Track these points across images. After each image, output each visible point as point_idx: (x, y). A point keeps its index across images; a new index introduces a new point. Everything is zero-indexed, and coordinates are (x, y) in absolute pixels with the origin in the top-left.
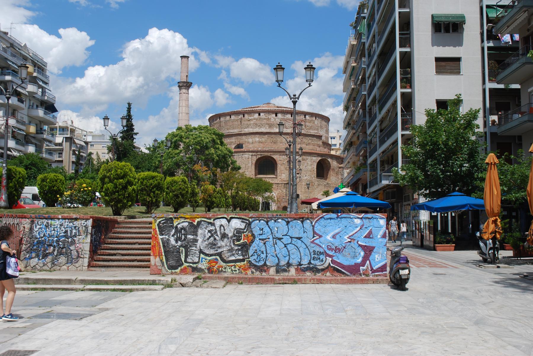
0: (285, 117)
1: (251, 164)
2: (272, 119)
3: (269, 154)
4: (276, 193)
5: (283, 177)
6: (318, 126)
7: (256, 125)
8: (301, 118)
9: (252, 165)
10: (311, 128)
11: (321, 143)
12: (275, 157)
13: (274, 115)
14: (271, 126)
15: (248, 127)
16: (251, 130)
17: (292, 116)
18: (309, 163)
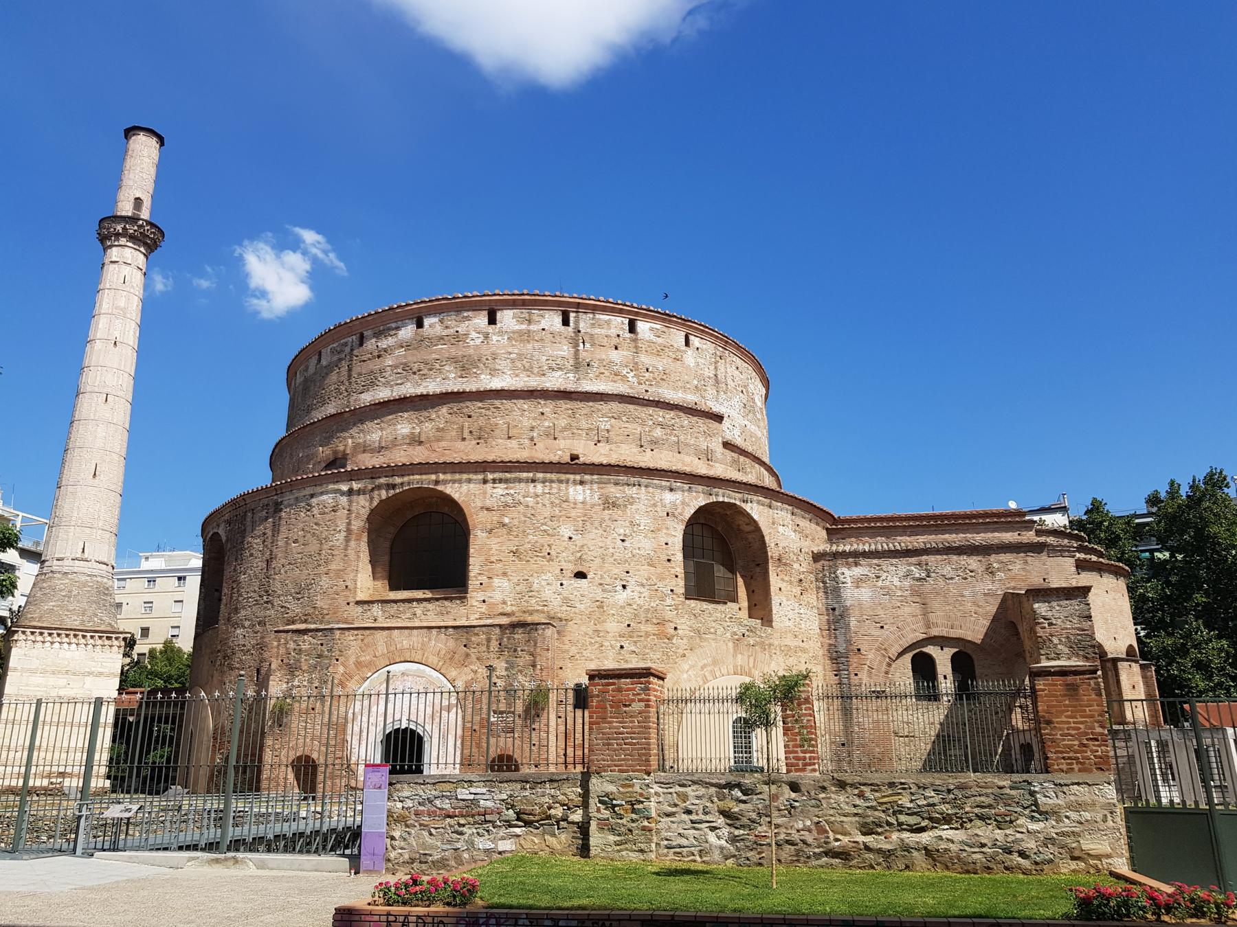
2: (474, 335)
3: (426, 481)
5: (498, 596)
6: (702, 378)
8: (613, 332)
9: (347, 540)
10: (664, 376)
11: (719, 449)
12: (460, 490)
13: (481, 320)
14: (466, 366)
15: (372, 384)
16: (383, 394)
17: (566, 322)
18: (644, 521)
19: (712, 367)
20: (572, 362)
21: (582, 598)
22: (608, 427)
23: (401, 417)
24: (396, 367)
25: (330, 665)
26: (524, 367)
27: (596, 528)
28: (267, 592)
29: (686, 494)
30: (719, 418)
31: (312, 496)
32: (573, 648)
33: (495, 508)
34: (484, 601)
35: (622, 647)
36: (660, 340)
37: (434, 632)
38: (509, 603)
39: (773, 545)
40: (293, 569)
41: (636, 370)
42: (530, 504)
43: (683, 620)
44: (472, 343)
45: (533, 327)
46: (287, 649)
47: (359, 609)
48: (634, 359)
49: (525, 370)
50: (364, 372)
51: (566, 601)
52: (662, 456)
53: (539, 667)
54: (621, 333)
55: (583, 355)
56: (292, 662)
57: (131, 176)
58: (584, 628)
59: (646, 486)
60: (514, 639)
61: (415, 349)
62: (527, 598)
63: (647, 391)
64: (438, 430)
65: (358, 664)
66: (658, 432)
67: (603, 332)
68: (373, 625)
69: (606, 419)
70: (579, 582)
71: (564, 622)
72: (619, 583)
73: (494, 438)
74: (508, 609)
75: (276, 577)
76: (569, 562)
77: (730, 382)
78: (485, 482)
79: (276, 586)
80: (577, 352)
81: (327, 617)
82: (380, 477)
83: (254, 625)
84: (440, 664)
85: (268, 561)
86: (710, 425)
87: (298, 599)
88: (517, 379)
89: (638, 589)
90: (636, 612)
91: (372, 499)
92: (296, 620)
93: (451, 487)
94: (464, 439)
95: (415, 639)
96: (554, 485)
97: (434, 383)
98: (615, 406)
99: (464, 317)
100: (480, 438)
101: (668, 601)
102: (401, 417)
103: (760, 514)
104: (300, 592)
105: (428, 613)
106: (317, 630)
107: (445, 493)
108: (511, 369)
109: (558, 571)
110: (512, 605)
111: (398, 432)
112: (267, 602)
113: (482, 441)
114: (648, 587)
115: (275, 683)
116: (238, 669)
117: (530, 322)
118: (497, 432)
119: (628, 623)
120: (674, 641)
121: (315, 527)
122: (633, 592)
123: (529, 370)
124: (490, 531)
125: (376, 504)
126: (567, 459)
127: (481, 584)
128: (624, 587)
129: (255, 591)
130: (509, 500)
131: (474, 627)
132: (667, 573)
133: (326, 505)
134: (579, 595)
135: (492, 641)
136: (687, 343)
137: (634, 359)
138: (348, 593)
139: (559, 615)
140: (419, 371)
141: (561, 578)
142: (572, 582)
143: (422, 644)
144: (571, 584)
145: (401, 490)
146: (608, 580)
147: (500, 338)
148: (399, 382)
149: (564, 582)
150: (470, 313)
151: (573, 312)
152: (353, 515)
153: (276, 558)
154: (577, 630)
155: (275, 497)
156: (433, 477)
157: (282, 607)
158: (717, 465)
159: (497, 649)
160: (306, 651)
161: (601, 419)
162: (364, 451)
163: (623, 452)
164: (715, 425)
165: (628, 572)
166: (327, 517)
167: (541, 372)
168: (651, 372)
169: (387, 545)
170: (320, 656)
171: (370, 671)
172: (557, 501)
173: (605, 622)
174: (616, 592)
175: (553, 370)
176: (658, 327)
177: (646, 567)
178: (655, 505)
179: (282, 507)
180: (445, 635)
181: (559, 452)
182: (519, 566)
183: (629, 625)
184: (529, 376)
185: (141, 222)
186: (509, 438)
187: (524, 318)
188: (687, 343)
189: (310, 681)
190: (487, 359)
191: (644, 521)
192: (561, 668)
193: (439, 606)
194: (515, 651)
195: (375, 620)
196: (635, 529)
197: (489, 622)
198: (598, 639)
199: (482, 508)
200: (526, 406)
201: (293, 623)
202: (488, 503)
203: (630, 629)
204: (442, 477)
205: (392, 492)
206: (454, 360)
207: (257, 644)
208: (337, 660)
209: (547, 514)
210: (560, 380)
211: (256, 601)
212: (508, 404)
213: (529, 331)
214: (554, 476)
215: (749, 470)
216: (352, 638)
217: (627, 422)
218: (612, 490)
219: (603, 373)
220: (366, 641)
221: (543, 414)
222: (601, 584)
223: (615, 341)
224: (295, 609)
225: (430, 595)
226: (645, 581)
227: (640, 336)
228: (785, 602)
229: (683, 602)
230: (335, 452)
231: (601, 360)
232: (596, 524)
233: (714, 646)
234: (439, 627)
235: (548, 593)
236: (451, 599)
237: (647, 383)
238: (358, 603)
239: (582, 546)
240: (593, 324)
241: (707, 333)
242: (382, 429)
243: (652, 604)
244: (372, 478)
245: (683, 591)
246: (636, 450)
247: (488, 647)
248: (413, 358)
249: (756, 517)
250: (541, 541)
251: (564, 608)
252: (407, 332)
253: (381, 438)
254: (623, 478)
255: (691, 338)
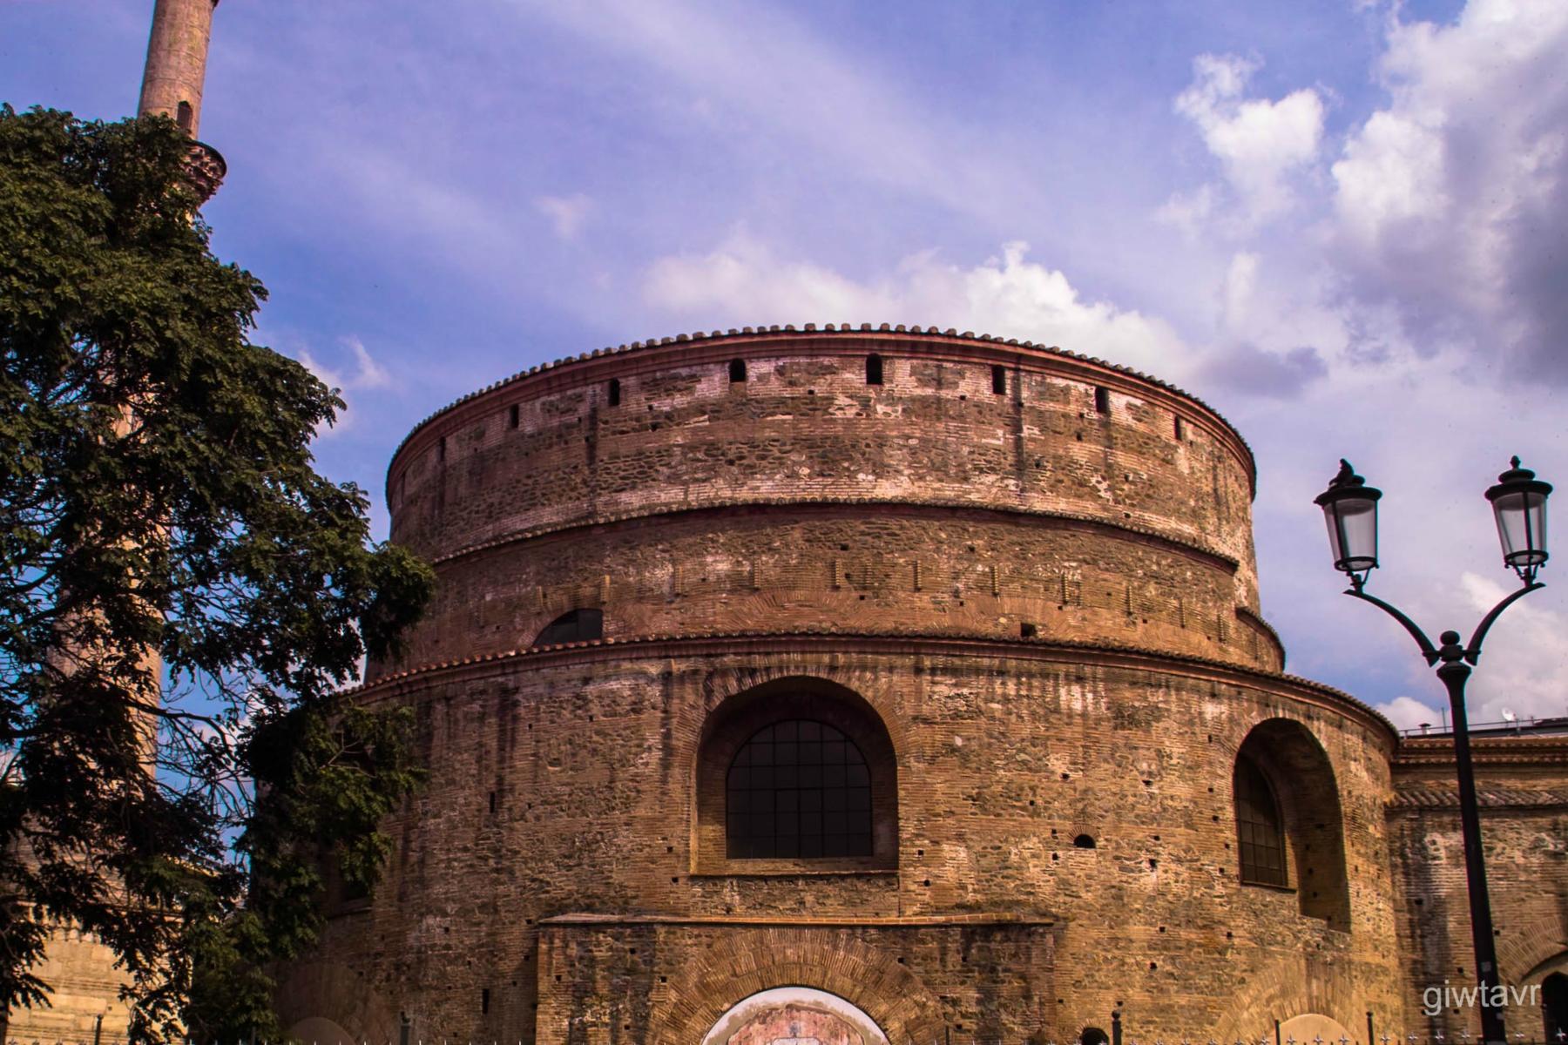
0: (946, 394)
1: (657, 755)
2: (842, 400)
3: (812, 665)
4: (895, 1025)
5: (949, 875)
6: (1199, 496)
7: (714, 457)
8: (1073, 409)
9: (665, 765)
10: (1148, 494)
11: (1232, 623)
13: (855, 377)
15: (642, 474)
16: (669, 496)
17: (998, 388)
18: (1176, 749)
19: (1210, 477)
20: (1011, 458)
21: (1088, 882)
22: (1078, 577)
23: (712, 540)
24: (693, 448)
25: (651, 989)
26: (933, 464)
27: (1106, 761)
28: (496, 851)
29: (1234, 705)
30: (1230, 565)
31: (586, 681)
32: (1079, 967)
33: (938, 720)
34: (927, 883)
35: (1153, 966)
36: (1141, 427)
37: (843, 934)
38: (970, 888)
39: (1345, 793)
40: (552, 812)
41: (1111, 478)
42: (997, 715)
43: (1239, 922)
44: (839, 414)
45: (946, 394)
46: (567, 957)
47: (698, 890)
48: (1106, 456)
49: (934, 468)
50: (623, 451)
51: (1064, 885)
52: (1160, 632)
53: (1036, 999)
54: (1085, 411)
55: (1031, 446)
56: (578, 980)
57: (174, 61)
58: (1094, 933)
59: (1178, 690)
60: (989, 950)
61: (730, 418)
62: (999, 879)
63: (1127, 516)
64: (786, 568)
65: (705, 988)
66: (1152, 590)
67: (1059, 407)
68: (727, 920)
69: (1074, 564)
70: (1083, 853)
71: (1062, 923)
72: (1144, 856)
73: (891, 590)
74: (970, 897)
75: (517, 825)
76: (1066, 818)
77: (1230, 498)
78: (918, 671)
79: (519, 839)
80: (1018, 443)
81: (635, 902)
82: (723, 655)
83: (469, 911)
84: (858, 990)
85: (492, 795)
86: (1221, 580)
87: (569, 868)
88: (922, 484)
89: (1173, 866)
90: (1172, 907)
91: (709, 693)
92: (567, 906)
93: (859, 679)
94: (836, 588)
95: (807, 946)
96: (1035, 683)
97: (770, 483)
98: (1086, 539)
99: (823, 367)
100: (865, 588)
101: (1217, 887)
102: (712, 540)
103: (1329, 739)
104: (577, 852)
105: (828, 902)
106: (622, 924)
107: (849, 691)
108: (910, 467)
109: (1048, 834)
110: (975, 891)
111: (709, 568)
112: (497, 871)
113: (869, 593)
114: (1187, 864)
115: (548, 1018)
116: (436, 988)
117: (939, 384)
118: (895, 580)
119: (1160, 924)
120: (1228, 956)
121: (595, 738)
122: (1166, 872)
123: (940, 470)
124: (932, 760)
125: (718, 703)
126: (1016, 631)
127: (921, 853)
128: (1153, 863)
129: (466, 849)
130: (961, 705)
131: (917, 927)
132: (1214, 841)
133: (618, 699)
134: (1083, 877)
135: (950, 954)
136: (1178, 434)
137: (1106, 456)
138: (673, 861)
139: (1053, 910)
140: (741, 458)
141: (1053, 846)
142: (1072, 853)
143: (823, 957)
144: (1071, 857)
145: (765, 679)
146: (1127, 852)
147: (889, 409)
148: (700, 475)
149: (1060, 853)
150: (835, 361)
151: (1010, 369)
152: (675, 721)
153: (512, 791)
154: (1082, 936)
155: (500, 679)
156: (826, 658)
157: (533, 880)
158: (1231, 649)
159: (958, 968)
160: (603, 962)
161: (1066, 564)
162: (640, 600)
163: (1102, 623)
164: (1223, 576)
165: (1157, 838)
166: (623, 721)
167: (962, 475)
168: (1132, 483)
169: (720, 775)
170: (629, 972)
171: (727, 1000)
172: (1041, 711)
173: (1128, 923)
174: (1141, 871)
175: (982, 471)
176: (1139, 403)
177: (1182, 830)
178: (1191, 723)
179: (519, 697)
180: (864, 940)
181: (1003, 620)
182: (984, 823)
183: (1162, 929)
184: (941, 480)
185: (197, 150)
186: (918, 590)
187: (929, 375)
188: (1178, 434)
189: (615, 1016)
190: (868, 446)
191: (1176, 749)
192: (1061, 1001)
193: (846, 890)
194: (993, 970)
195: (729, 910)
196: (1165, 764)
197: (940, 919)
198: (1117, 952)
199: (915, 718)
200: (943, 535)
201: (563, 910)
202: (925, 709)
203: (1164, 936)
204: (841, 659)
205: (748, 683)
206: (808, 444)
207: (482, 946)
208: (664, 980)
209: (1026, 732)
210: (994, 490)
211: (471, 866)
212: (912, 527)
213: (939, 400)
214: (1035, 666)
215: (1266, 659)
216: (690, 942)
217: (1107, 570)
218: (1127, 694)
219: (1061, 481)
220: (717, 946)
221: (972, 549)
222: (1117, 858)
223: (1076, 425)
224: (562, 883)
225: (797, 870)
226: (1182, 854)
227: (1114, 418)
228: (1364, 892)
229: (1239, 890)
230: (575, 599)
231: (1057, 458)
232: (1106, 751)
233: (1282, 965)
234: (852, 927)
235: (1033, 871)
236: (868, 878)
237: (1128, 501)
238: (693, 878)
239: (1085, 791)
240: (1041, 393)
241: (1203, 416)
242: (674, 562)
243: (1196, 894)
244: (709, 656)
245: (1234, 870)
246: (1122, 620)
247: (943, 961)
248: (728, 434)
249: (1324, 745)
250: (1018, 780)
251: (1061, 899)
252: (713, 385)
253: (673, 576)
254: (1142, 671)
255: (1183, 423)
